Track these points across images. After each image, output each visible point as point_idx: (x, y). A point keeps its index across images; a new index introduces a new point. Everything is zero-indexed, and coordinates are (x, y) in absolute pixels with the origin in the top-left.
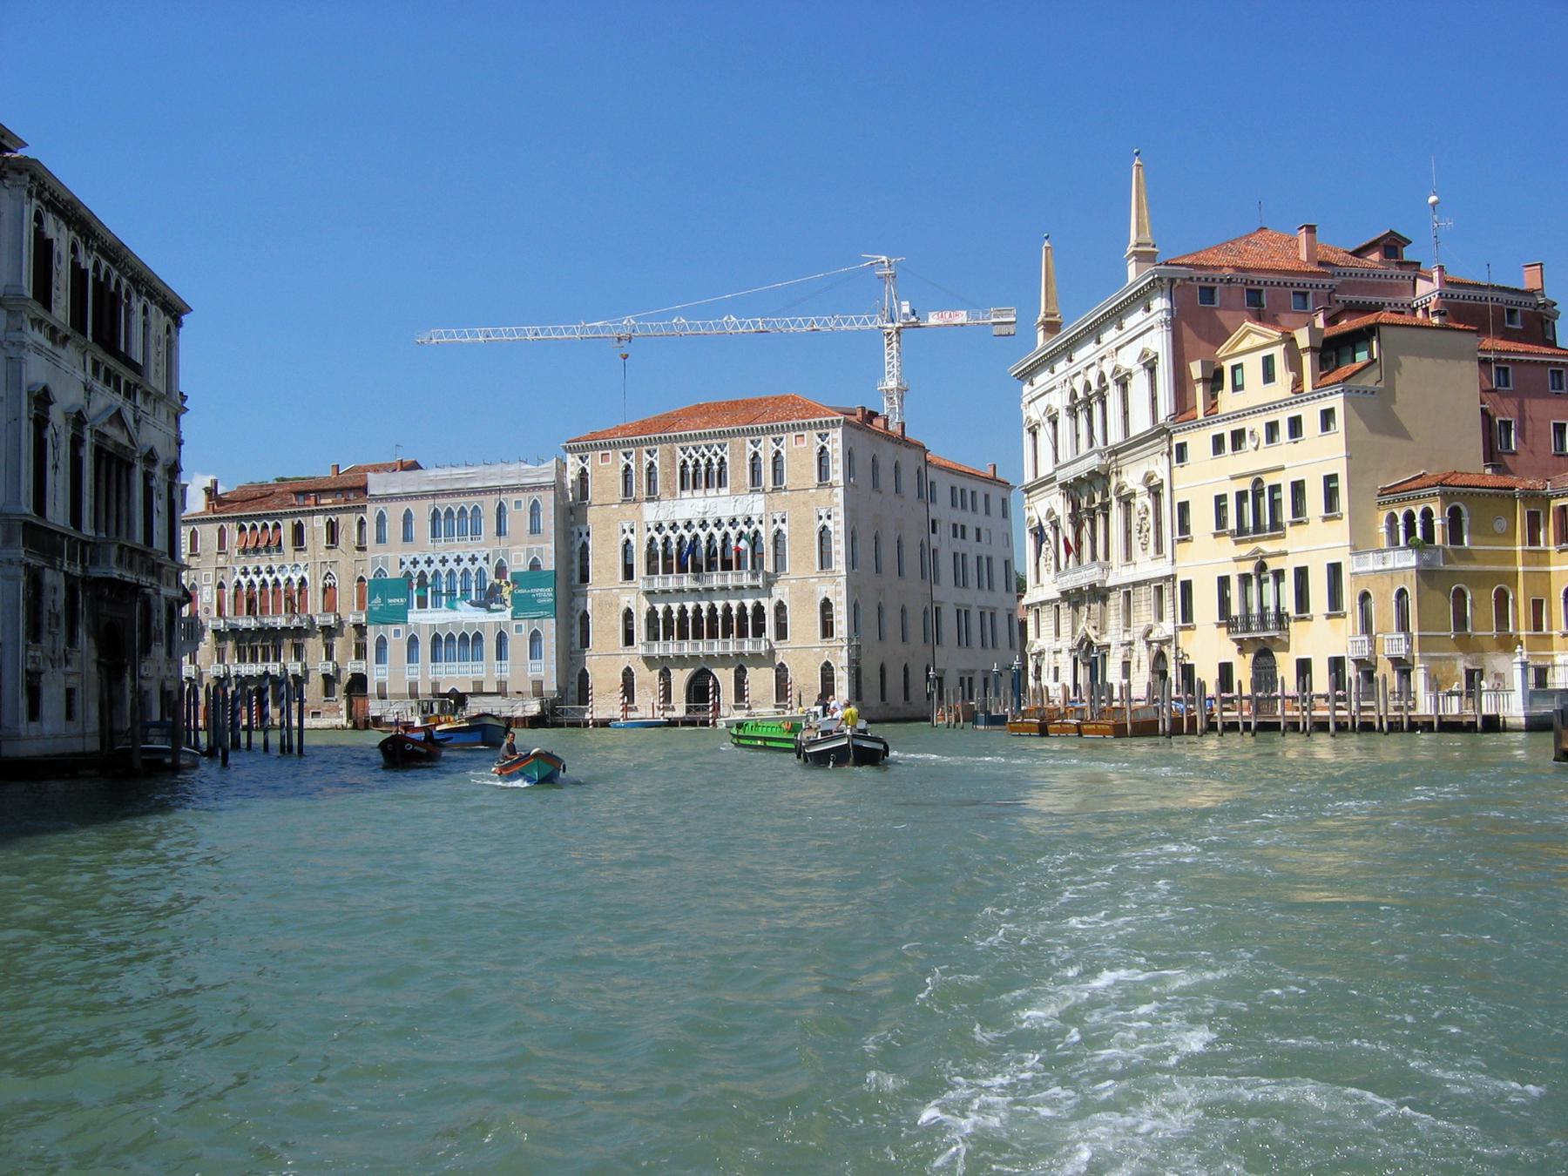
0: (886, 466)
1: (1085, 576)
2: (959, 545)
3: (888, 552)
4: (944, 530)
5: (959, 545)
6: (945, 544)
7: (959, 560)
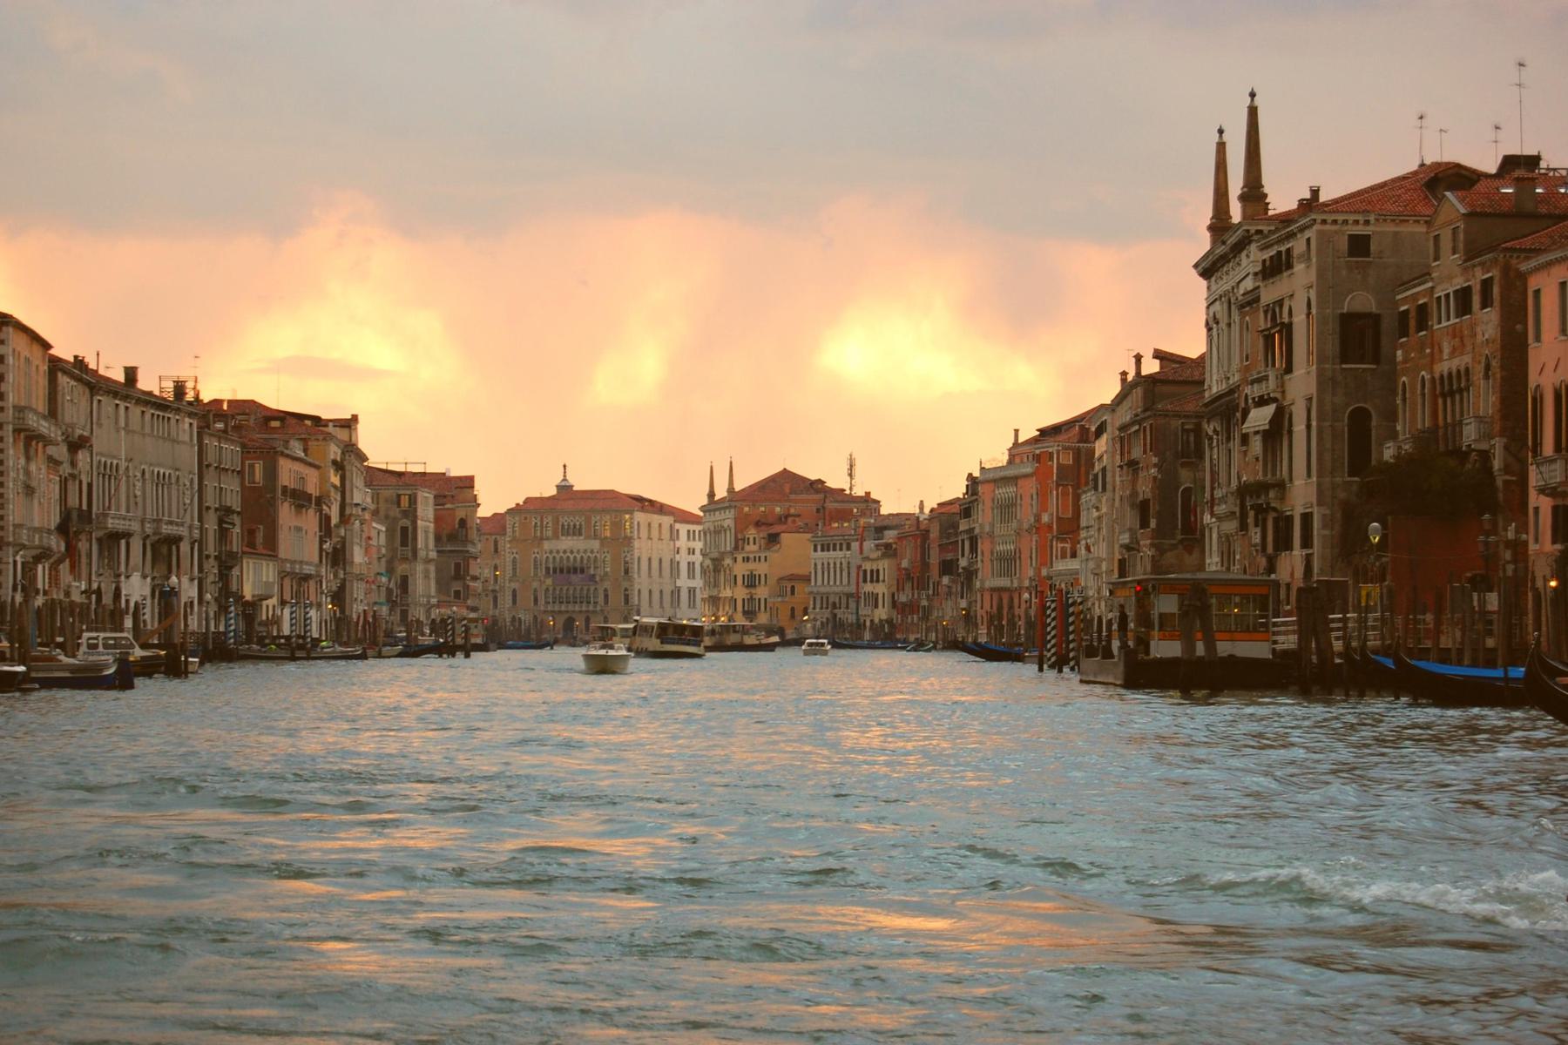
0: (655, 526)
1: (714, 593)
2: (692, 558)
3: (655, 564)
4: (684, 552)
5: (692, 558)
6: (683, 559)
7: (691, 565)
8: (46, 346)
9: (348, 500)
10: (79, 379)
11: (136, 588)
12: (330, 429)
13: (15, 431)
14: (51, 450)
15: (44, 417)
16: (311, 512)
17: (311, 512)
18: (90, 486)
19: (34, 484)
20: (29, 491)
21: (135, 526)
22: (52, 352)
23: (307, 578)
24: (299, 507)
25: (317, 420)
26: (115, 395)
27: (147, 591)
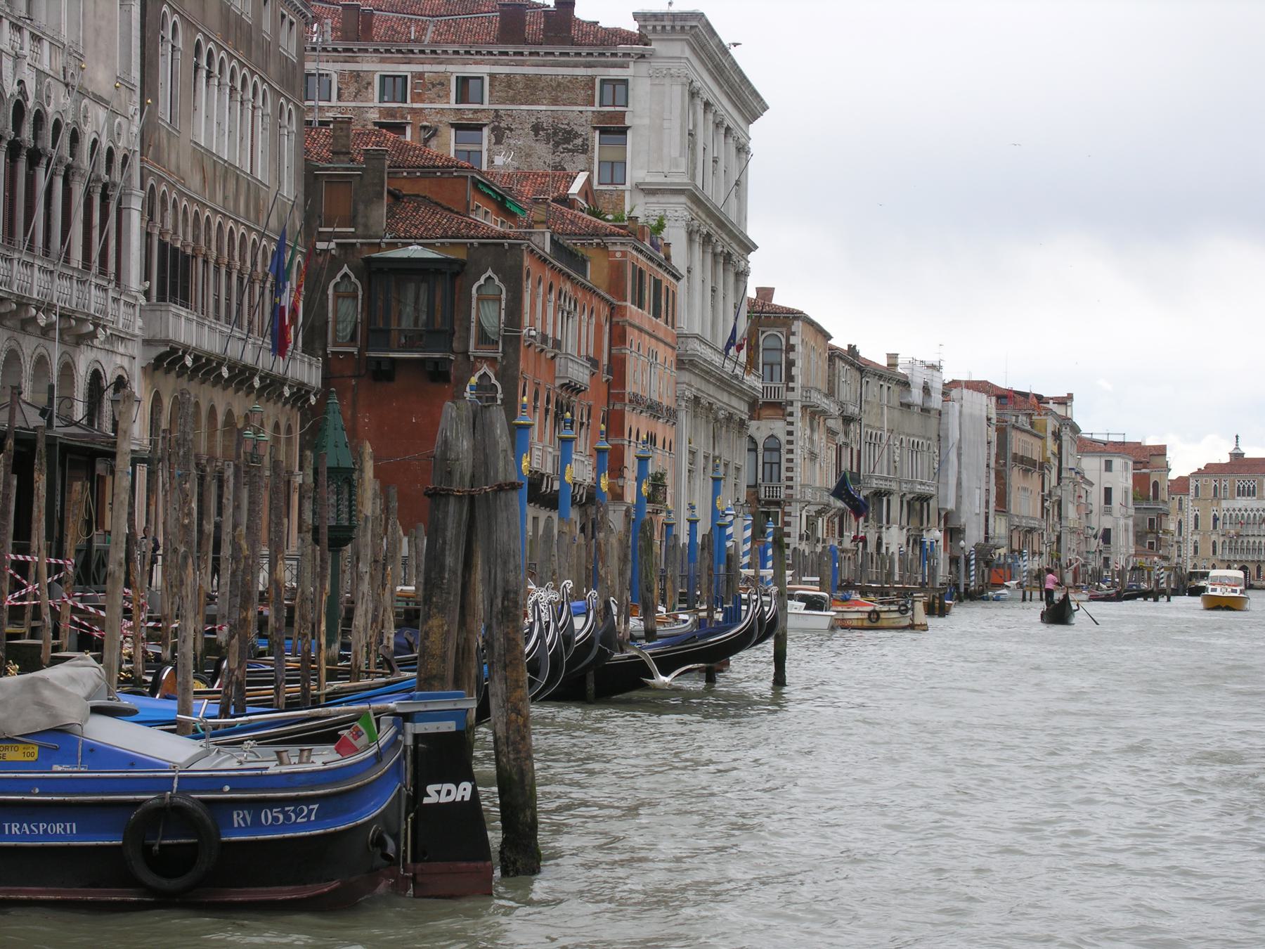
8: (827, 337)
9: (1064, 465)
10: (852, 365)
11: (895, 539)
12: (1051, 406)
13: (803, 407)
14: (831, 423)
15: (827, 396)
16: (1036, 475)
17: (1036, 475)
18: (859, 452)
19: (817, 451)
20: (813, 456)
21: (894, 486)
22: (831, 342)
23: (1031, 530)
24: (1026, 471)
25: (1039, 398)
26: (881, 377)
27: (904, 541)
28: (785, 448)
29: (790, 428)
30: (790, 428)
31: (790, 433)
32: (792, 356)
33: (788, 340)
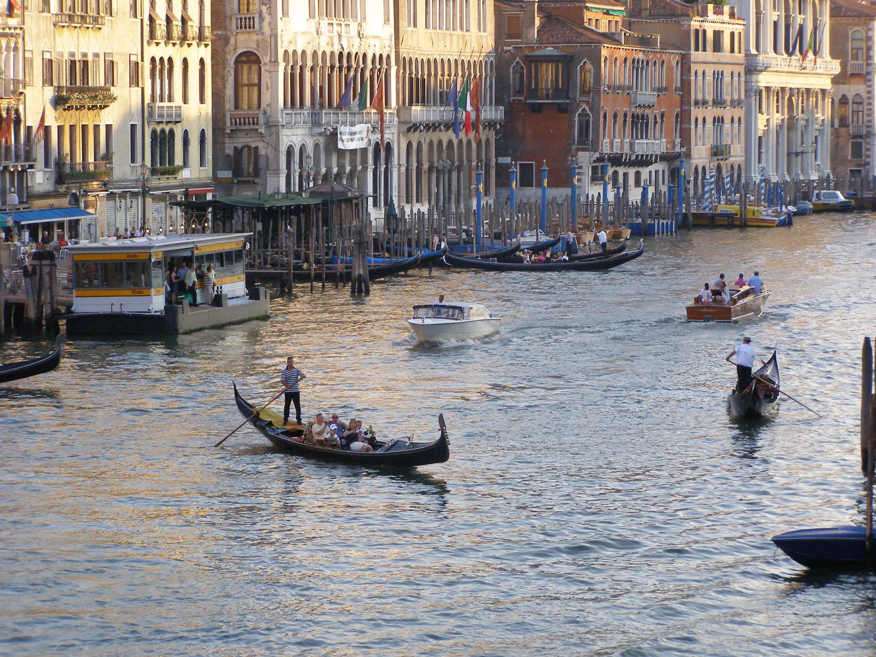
28: (866, 102)
29: (869, 89)
30: (869, 89)
31: (869, 92)
32: (870, 43)
33: (867, 33)
